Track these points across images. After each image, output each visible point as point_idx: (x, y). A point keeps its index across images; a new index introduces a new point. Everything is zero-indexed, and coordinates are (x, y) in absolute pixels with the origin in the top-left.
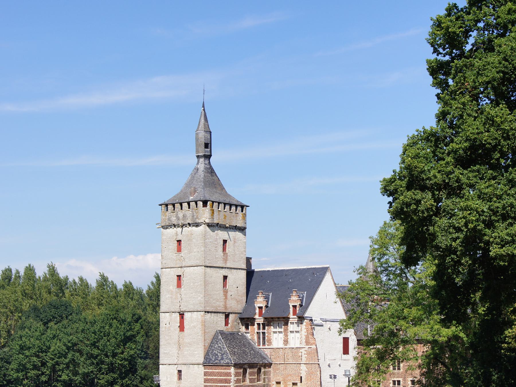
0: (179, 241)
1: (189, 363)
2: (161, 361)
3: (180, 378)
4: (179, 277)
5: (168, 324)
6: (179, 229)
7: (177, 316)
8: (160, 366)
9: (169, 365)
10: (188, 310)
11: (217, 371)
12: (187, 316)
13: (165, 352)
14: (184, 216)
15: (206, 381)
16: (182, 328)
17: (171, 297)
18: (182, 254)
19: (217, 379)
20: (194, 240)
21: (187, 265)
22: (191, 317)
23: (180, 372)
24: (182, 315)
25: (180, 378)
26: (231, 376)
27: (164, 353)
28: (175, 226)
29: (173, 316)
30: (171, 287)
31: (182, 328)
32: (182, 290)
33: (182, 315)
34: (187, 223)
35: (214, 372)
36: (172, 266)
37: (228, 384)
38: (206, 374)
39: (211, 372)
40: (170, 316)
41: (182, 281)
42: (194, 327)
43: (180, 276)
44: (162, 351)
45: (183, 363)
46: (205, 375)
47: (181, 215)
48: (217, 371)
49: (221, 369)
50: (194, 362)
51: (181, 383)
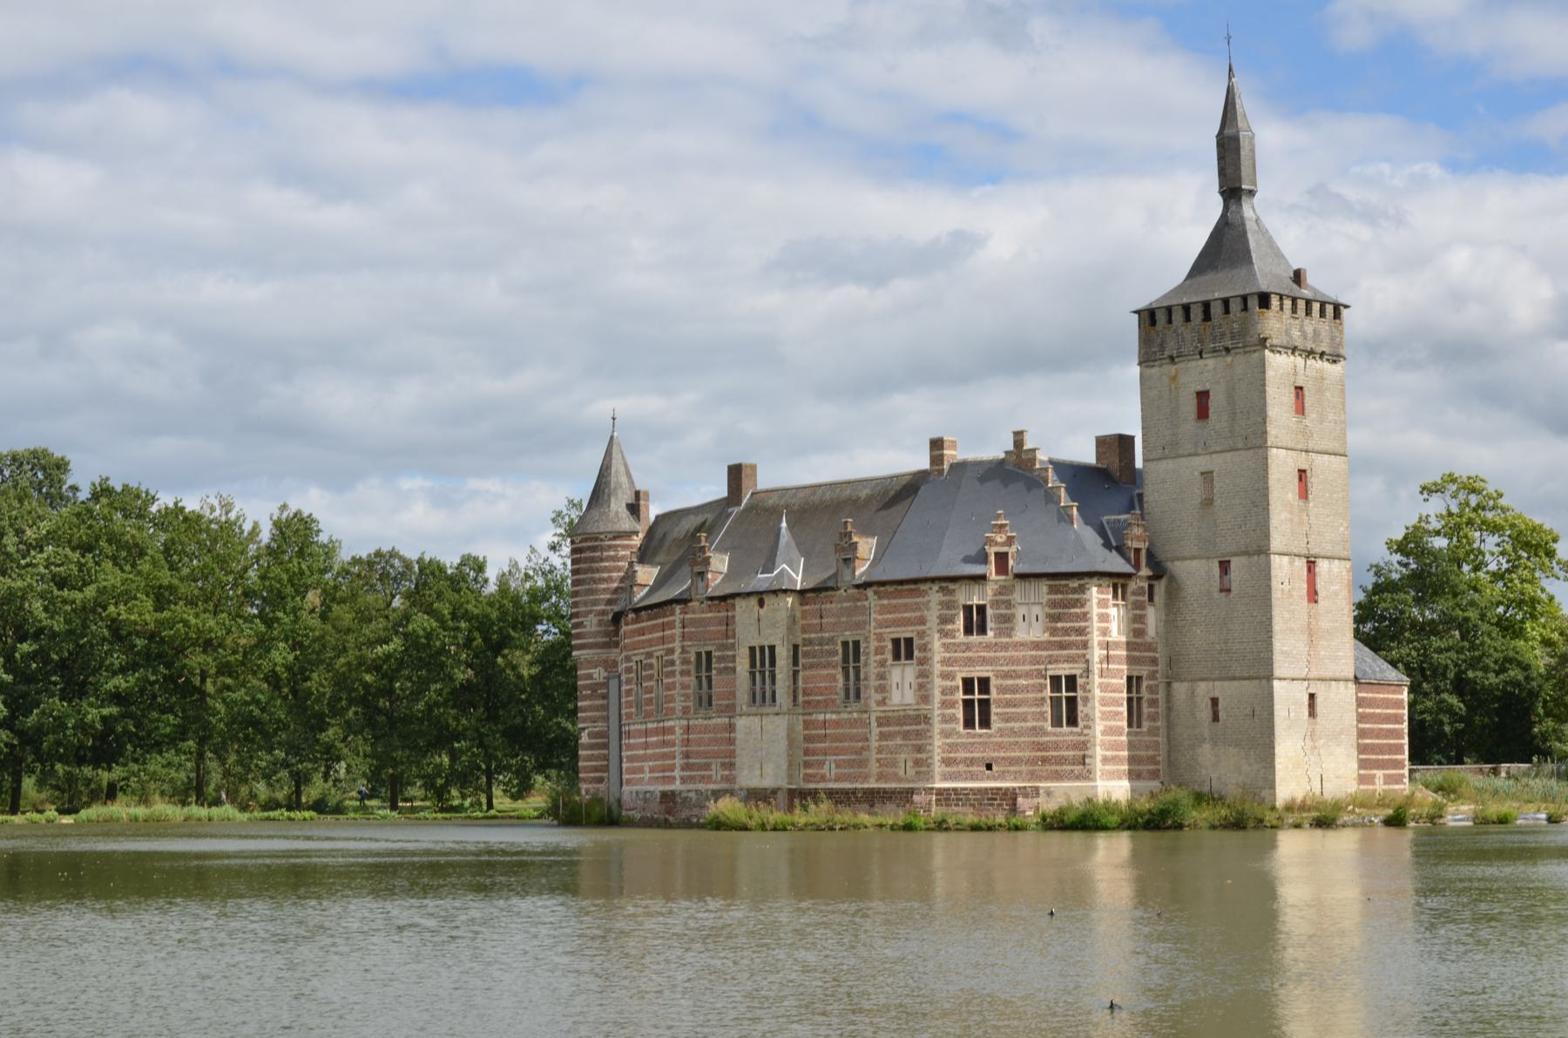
0: (1299, 389)
1: (1328, 677)
2: (1277, 672)
3: (1312, 712)
4: (1302, 472)
5: (1286, 583)
6: (1299, 361)
7: (1301, 564)
8: (1276, 683)
9: (1293, 680)
10: (1322, 554)
11: (1382, 696)
12: (1323, 566)
13: (1284, 649)
14: (1316, 333)
15: (1361, 718)
16: (1313, 595)
17: (1291, 520)
18: (1307, 422)
19: (1379, 714)
20: (1328, 394)
21: (1317, 448)
22: (1330, 571)
23: (1312, 696)
24: (1311, 565)
25: (1312, 712)
26: (1404, 708)
27: (1282, 652)
28: (1294, 350)
29: (1297, 564)
30: (1290, 495)
31: (1313, 595)
32: (1311, 505)
33: (1311, 565)
34: (1319, 350)
35: (1375, 698)
36: (1289, 446)
37: (1397, 726)
38: (1360, 703)
39: (1371, 699)
40: (1291, 563)
41: (1309, 485)
42: (1336, 594)
43: (1304, 471)
44: (1278, 645)
45: (1320, 677)
46: (1359, 706)
47: (1309, 329)
48: (1382, 696)
49: (1388, 693)
50: (1337, 675)
51: (1316, 724)
